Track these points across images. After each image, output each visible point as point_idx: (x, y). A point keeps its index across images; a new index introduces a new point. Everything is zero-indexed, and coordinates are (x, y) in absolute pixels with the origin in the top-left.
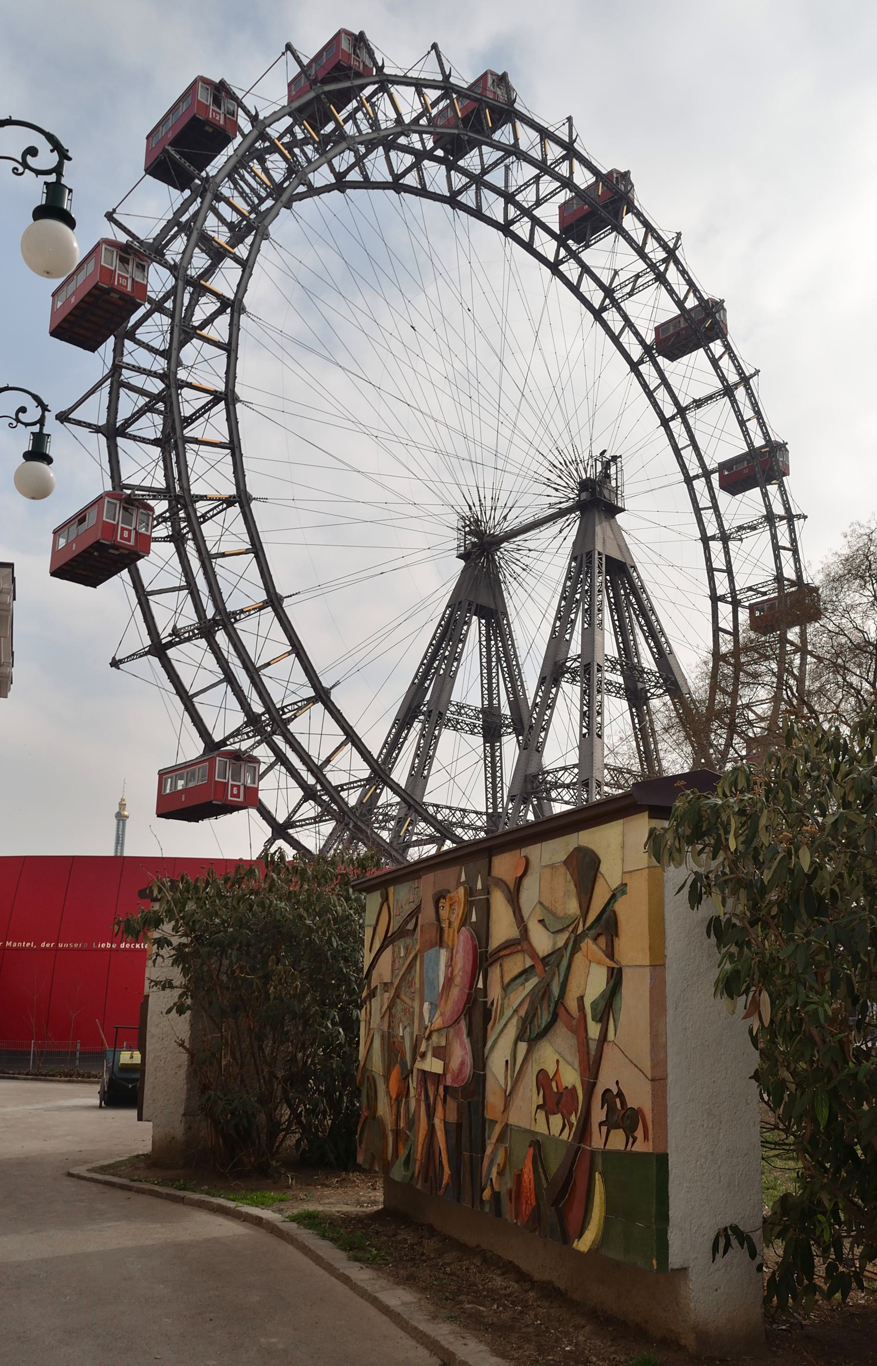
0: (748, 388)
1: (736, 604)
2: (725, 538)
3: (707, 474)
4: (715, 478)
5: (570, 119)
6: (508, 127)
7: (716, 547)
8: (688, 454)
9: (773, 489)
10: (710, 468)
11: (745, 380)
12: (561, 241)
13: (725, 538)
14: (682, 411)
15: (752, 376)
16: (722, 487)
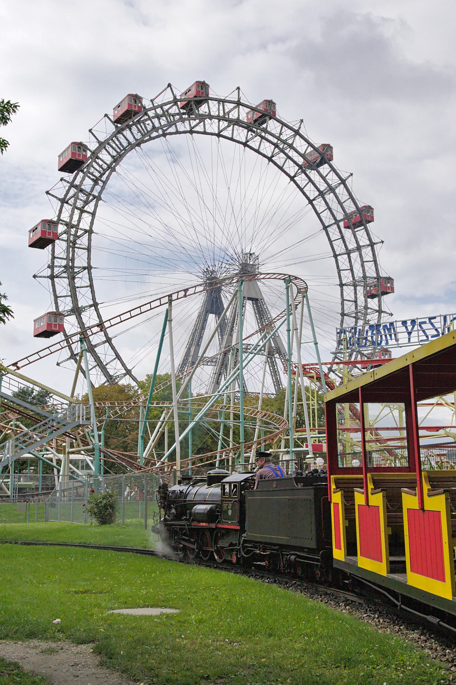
0: (346, 187)
1: (355, 286)
2: (348, 253)
3: (337, 222)
4: (342, 224)
5: (238, 88)
6: (206, 105)
7: (343, 259)
8: (326, 216)
9: (361, 233)
10: (338, 219)
11: (343, 182)
12: (248, 128)
13: (348, 253)
14: (322, 194)
15: (348, 178)
16: (347, 227)
